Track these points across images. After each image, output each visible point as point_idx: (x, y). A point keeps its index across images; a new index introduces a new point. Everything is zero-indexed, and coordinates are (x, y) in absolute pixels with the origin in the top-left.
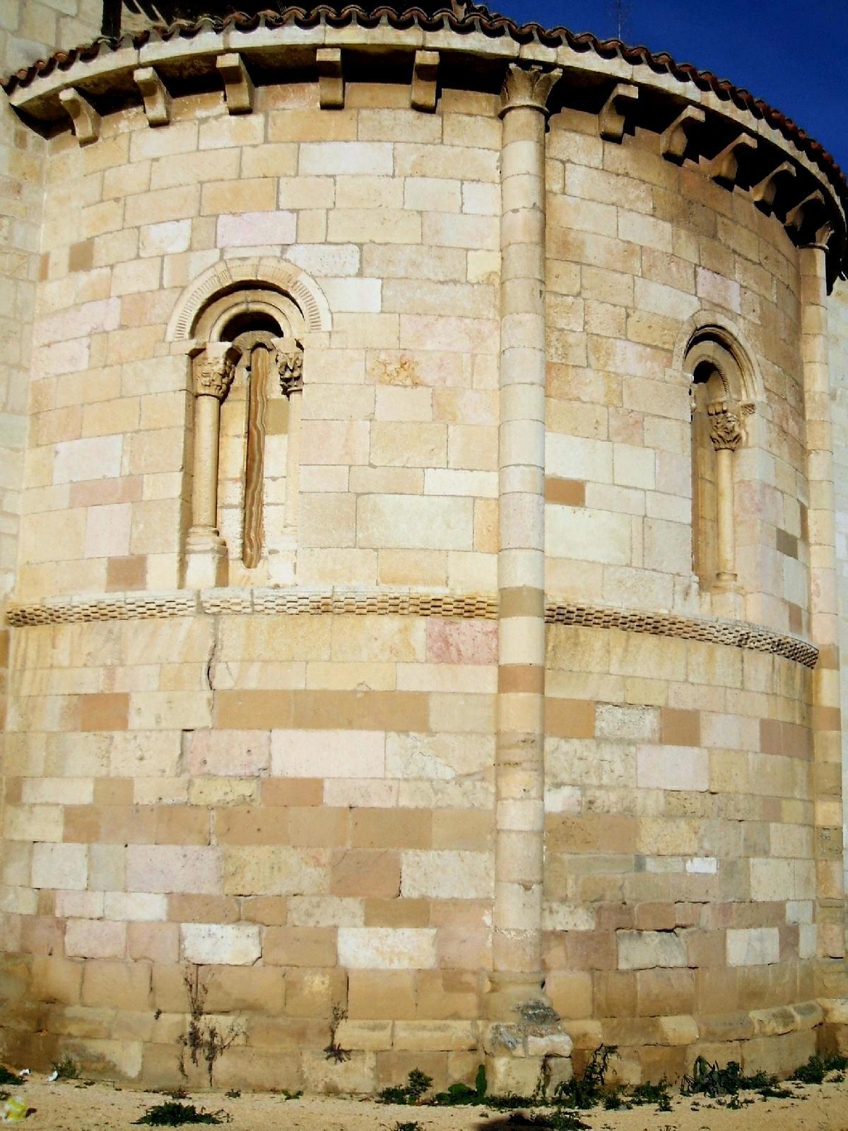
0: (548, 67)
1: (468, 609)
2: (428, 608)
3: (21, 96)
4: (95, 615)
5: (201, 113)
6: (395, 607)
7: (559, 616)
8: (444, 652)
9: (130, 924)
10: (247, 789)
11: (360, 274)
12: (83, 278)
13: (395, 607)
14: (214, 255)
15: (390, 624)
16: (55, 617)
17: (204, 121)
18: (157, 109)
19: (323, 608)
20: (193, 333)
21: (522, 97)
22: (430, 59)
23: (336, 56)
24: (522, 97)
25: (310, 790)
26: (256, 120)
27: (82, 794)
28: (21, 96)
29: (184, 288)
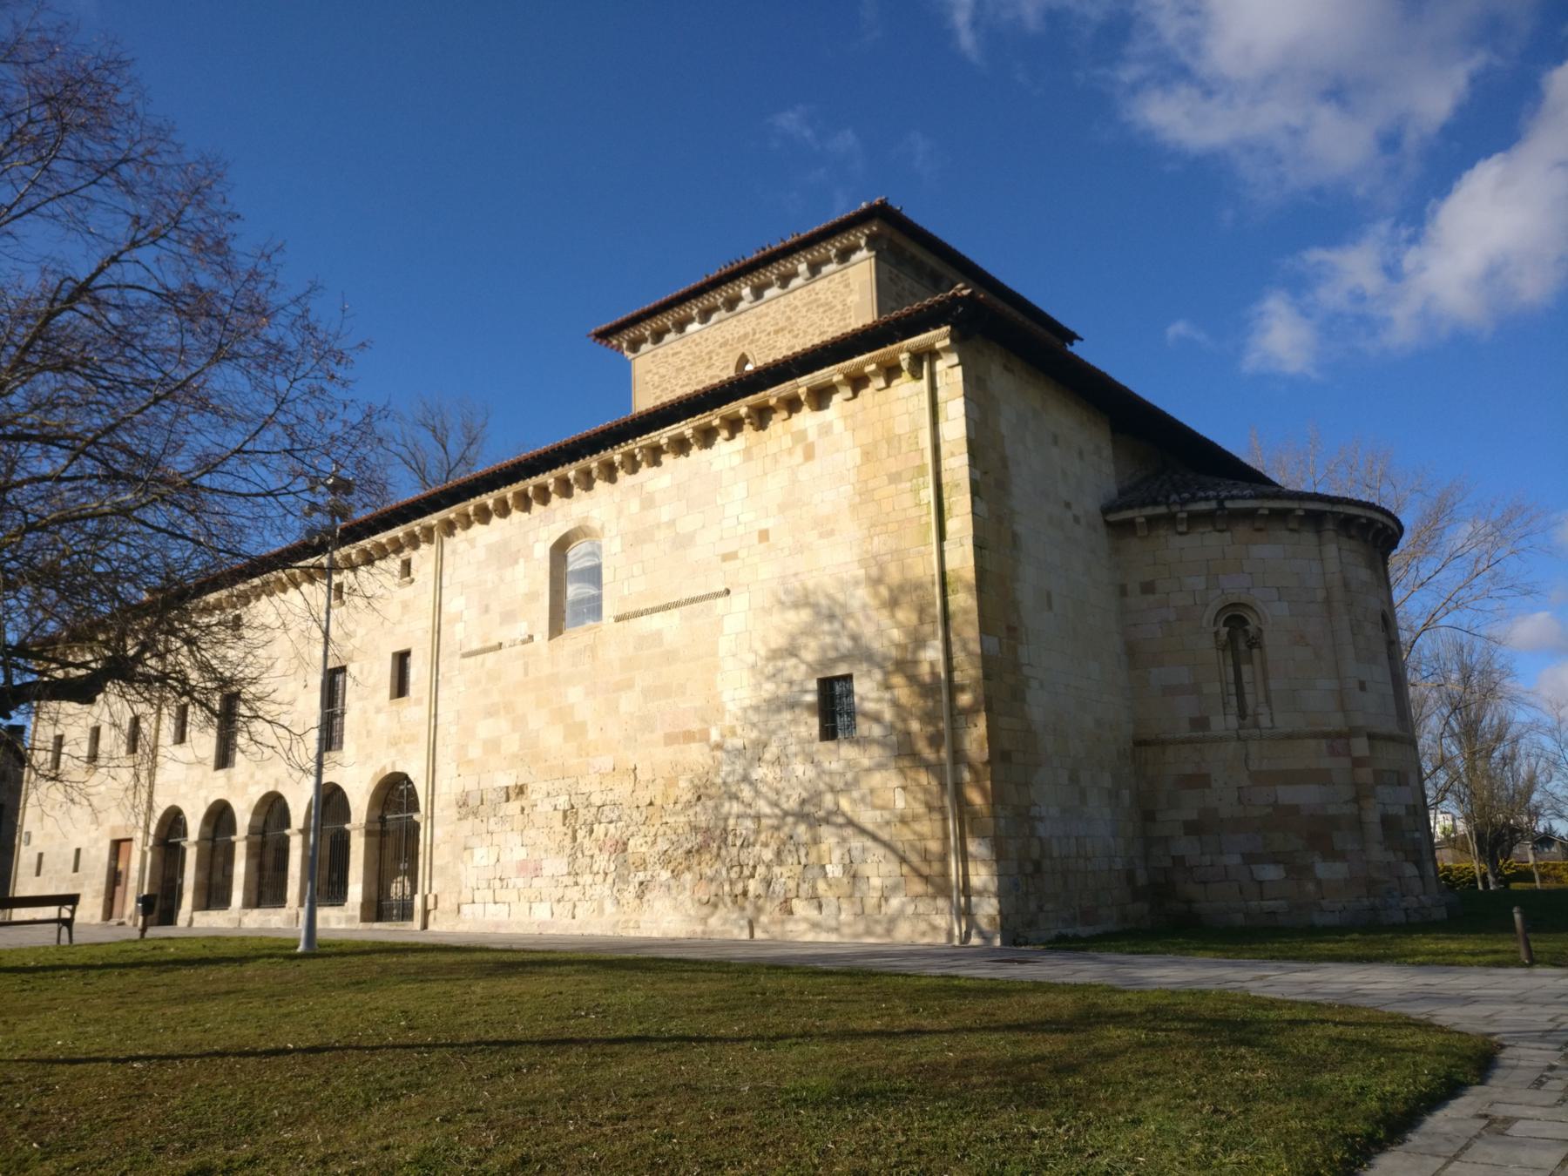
0: (1339, 513)
1: (1339, 735)
2: (1326, 735)
3: (1112, 518)
4: (1190, 741)
5: (1201, 530)
6: (1315, 736)
7: (1372, 737)
8: (1333, 752)
9: (1225, 866)
10: (1270, 810)
11: (1279, 600)
12: (1151, 598)
13: (1315, 736)
14: (1219, 592)
15: (1312, 743)
16: (1164, 743)
17: (1203, 533)
18: (1182, 528)
19: (1290, 737)
20: (1215, 624)
21: (1330, 525)
22: (1301, 513)
23: (1266, 512)
24: (1330, 525)
25: (1294, 809)
26: (1228, 535)
27: (1194, 816)
28: (1112, 518)
29: (1207, 605)
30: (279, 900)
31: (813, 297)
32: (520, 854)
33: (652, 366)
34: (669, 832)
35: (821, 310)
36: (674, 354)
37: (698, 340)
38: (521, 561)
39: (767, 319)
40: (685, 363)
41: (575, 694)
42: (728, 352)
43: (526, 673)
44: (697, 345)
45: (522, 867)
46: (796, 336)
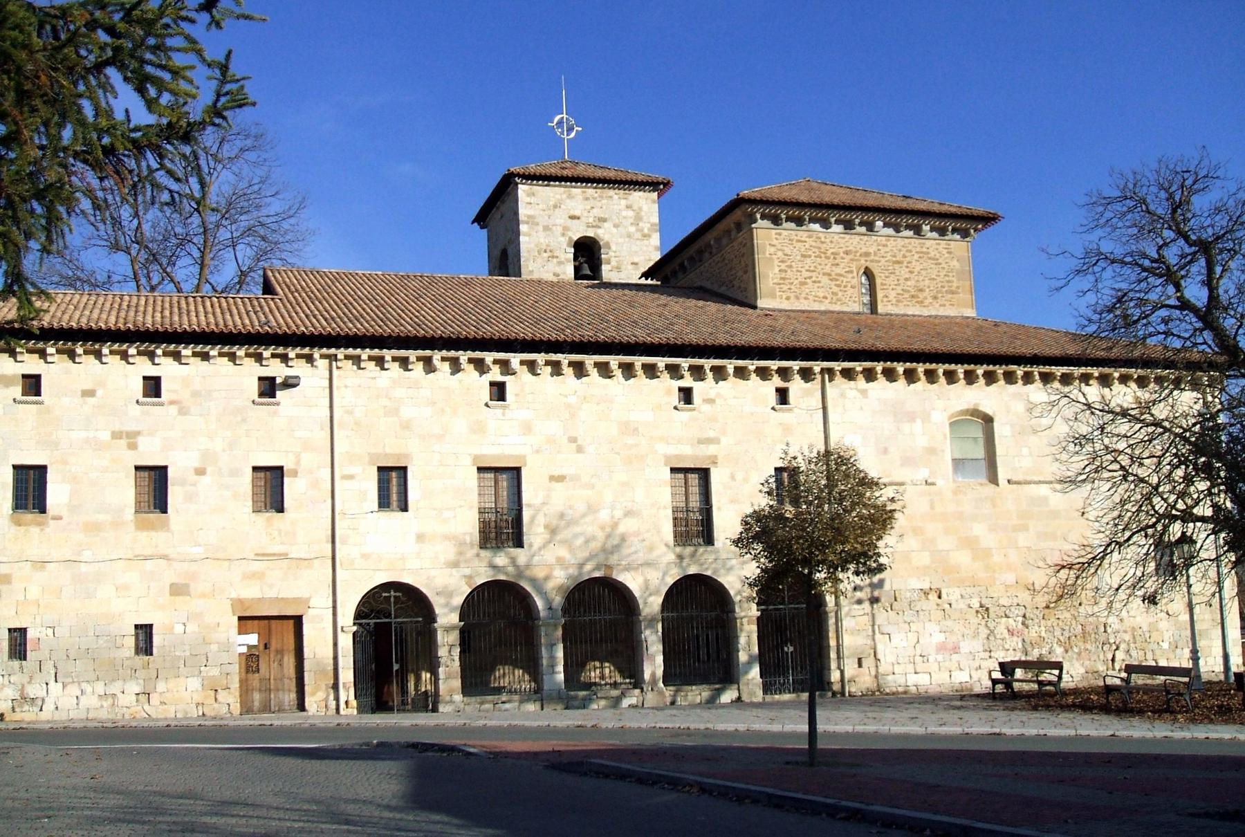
30: (727, 674)
31: (924, 250)
32: (939, 638)
33: (775, 242)
34: (1061, 623)
35: (930, 261)
36: (799, 241)
37: (823, 239)
38: (919, 421)
39: (887, 249)
40: (810, 253)
41: (979, 530)
42: (852, 260)
43: (932, 508)
44: (822, 243)
45: (941, 648)
46: (911, 272)
